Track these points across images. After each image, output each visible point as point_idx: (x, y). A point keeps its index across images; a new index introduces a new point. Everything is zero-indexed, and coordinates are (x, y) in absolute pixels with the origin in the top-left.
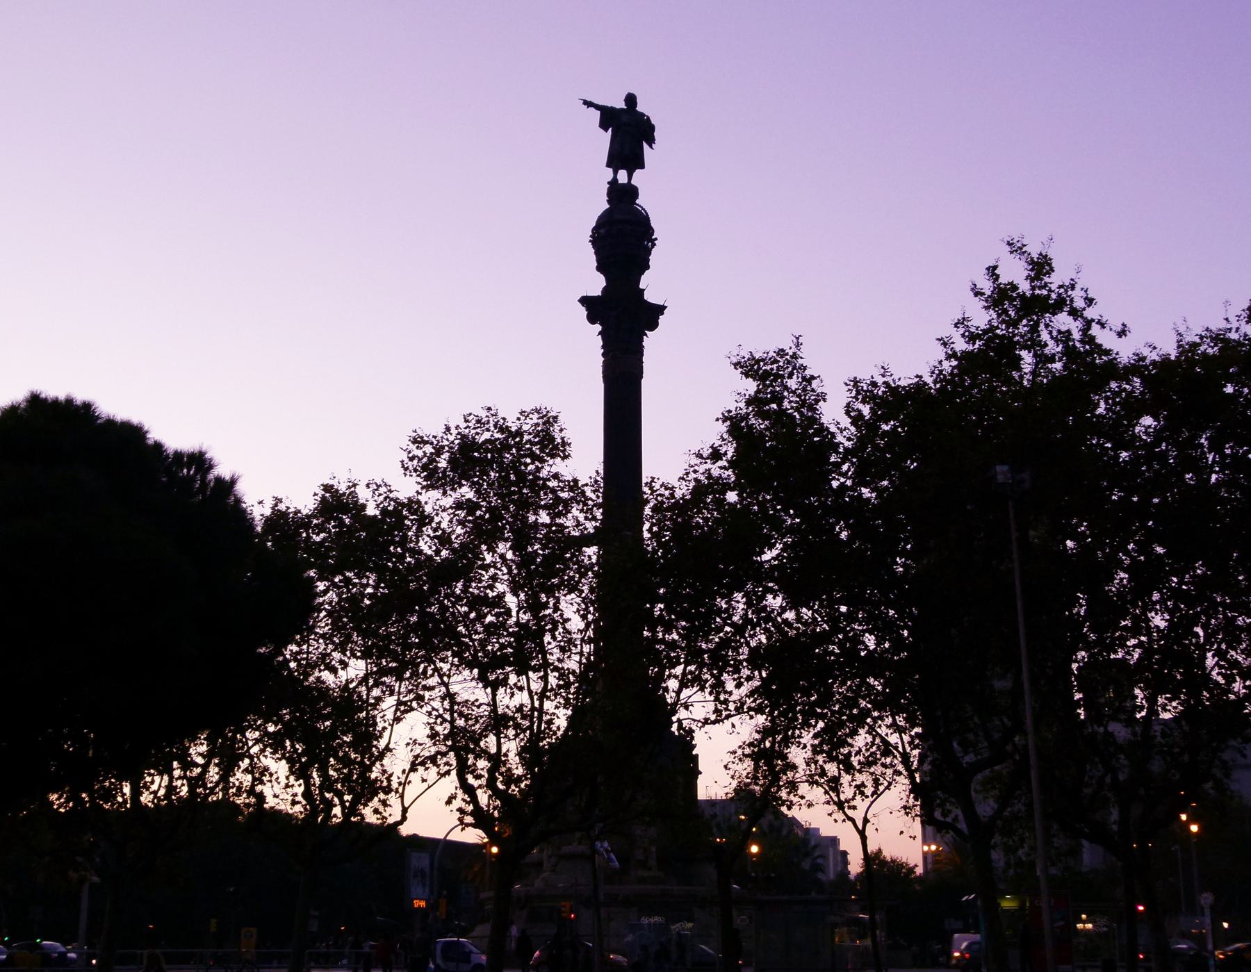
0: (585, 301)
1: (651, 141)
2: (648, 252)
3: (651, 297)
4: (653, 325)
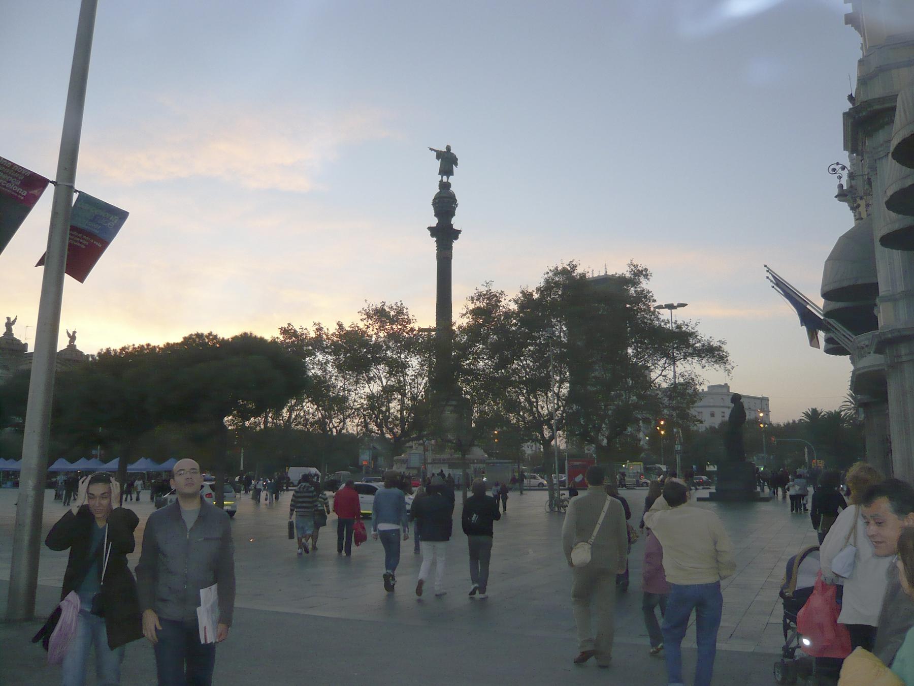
0: (430, 228)
1: (456, 164)
2: (455, 209)
3: (455, 227)
4: (456, 238)
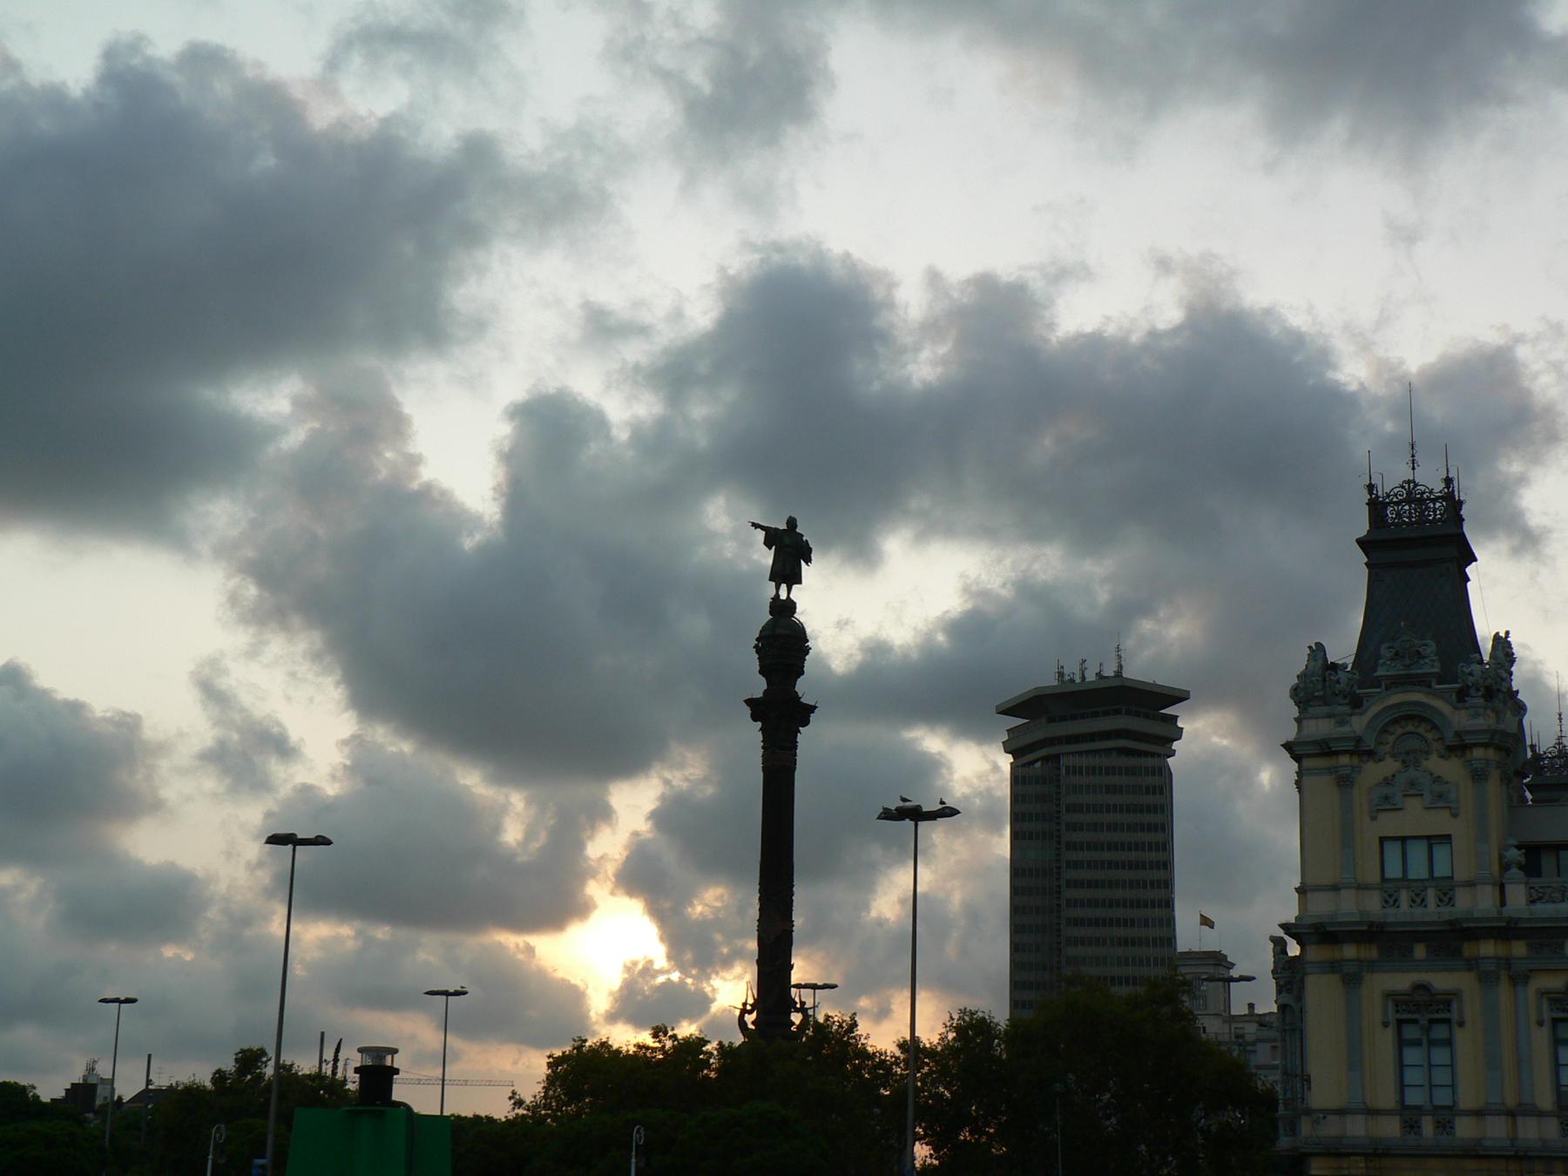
0: (749, 702)
1: (808, 561)
4: (806, 723)
